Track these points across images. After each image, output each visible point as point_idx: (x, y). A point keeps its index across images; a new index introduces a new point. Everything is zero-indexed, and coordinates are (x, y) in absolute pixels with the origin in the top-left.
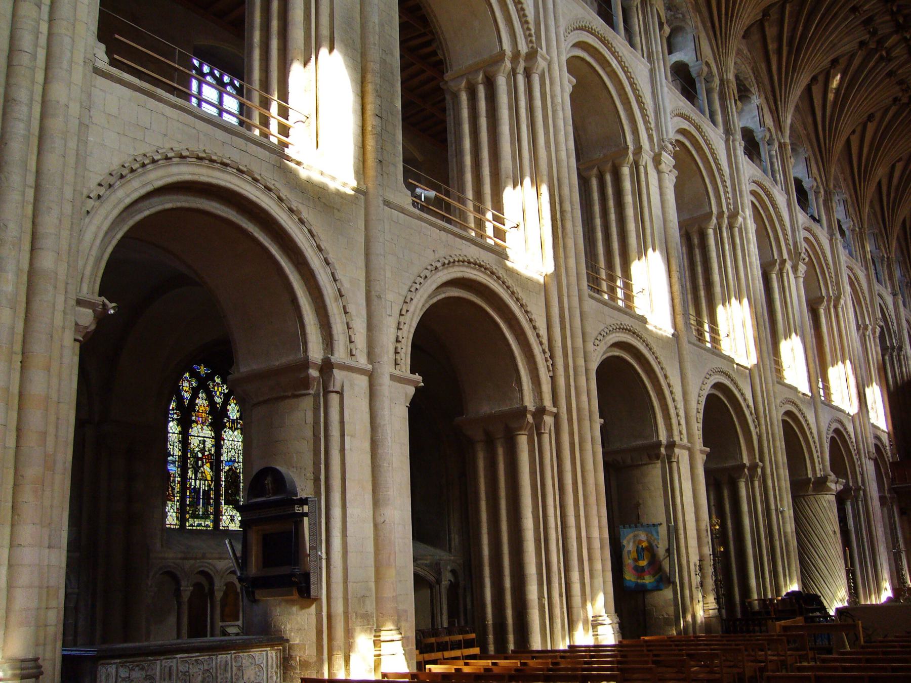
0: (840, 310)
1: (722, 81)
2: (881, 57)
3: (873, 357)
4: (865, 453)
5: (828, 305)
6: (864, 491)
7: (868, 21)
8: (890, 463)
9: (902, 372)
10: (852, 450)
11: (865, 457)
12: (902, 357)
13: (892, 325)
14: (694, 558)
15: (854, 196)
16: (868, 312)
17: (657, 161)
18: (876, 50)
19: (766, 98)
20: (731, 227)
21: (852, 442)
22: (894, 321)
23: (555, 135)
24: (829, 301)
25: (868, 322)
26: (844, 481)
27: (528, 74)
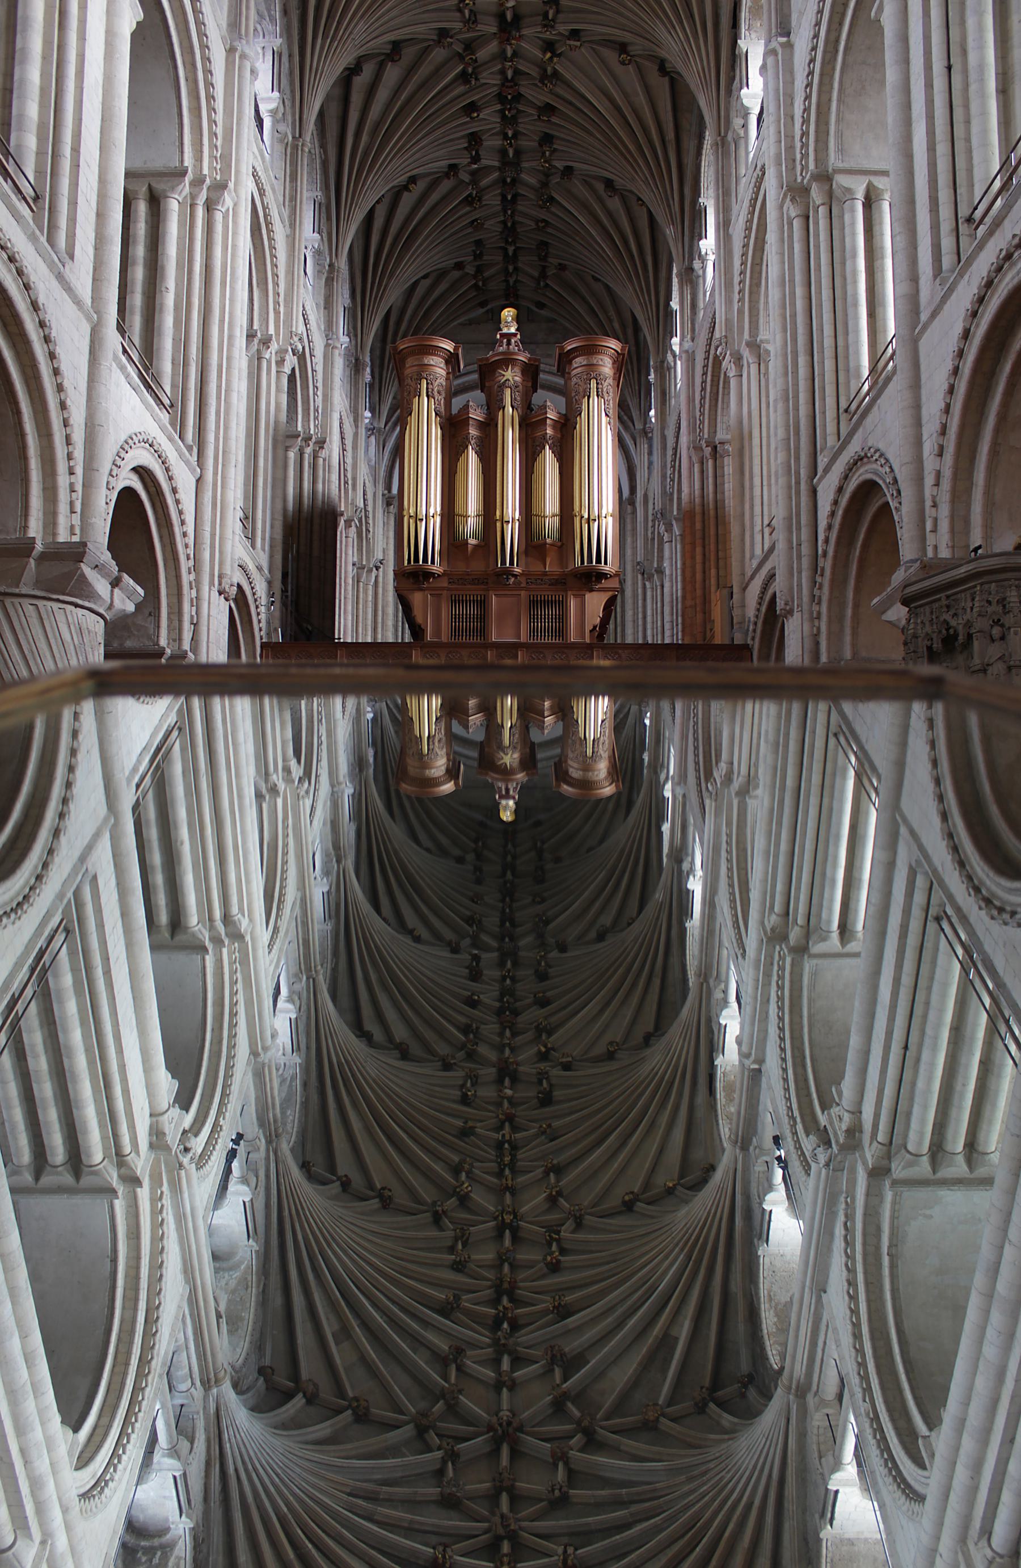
0: (219, 217)
3: (268, 412)
4: (212, 575)
5: (193, 197)
8: (263, 646)
9: (314, 492)
10: (182, 558)
11: (212, 583)
12: (321, 461)
13: (315, 394)
15: (297, 59)
16: (277, 313)
21: (185, 535)
22: (320, 385)
24: (198, 182)
25: (272, 331)
26: (141, 591)
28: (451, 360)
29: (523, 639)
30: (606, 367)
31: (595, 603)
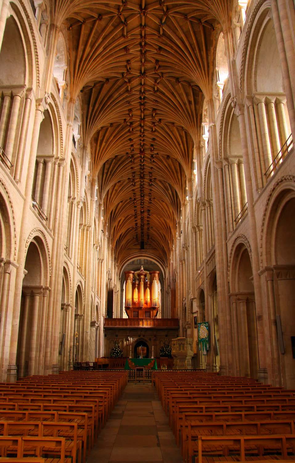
0: (102, 264)
1: (93, 179)
2: (132, 184)
6: (100, 327)
7: (134, 173)
14: (69, 346)
17: (78, 204)
18: (132, 182)
19: (99, 187)
20: (87, 230)
23: (64, 190)
27: (59, 166)
28: (133, 274)
29: (144, 318)
30: (157, 275)
31: (155, 312)
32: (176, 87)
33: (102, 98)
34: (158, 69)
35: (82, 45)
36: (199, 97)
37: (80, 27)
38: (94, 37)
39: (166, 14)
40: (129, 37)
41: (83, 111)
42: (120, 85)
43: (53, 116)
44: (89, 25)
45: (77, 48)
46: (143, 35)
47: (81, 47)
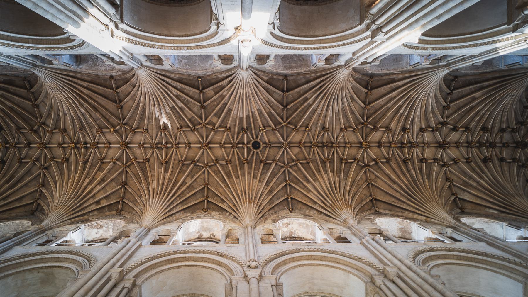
32: (114, 184)
33: (97, 99)
34: (137, 161)
35: (181, 87)
36: (109, 211)
37: (198, 88)
38: (185, 98)
39: (206, 165)
40: (179, 133)
41: (84, 73)
42: (111, 120)
43: (163, 39)
44: (196, 96)
45: (179, 81)
46: (180, 145)
47: (179, 85)
